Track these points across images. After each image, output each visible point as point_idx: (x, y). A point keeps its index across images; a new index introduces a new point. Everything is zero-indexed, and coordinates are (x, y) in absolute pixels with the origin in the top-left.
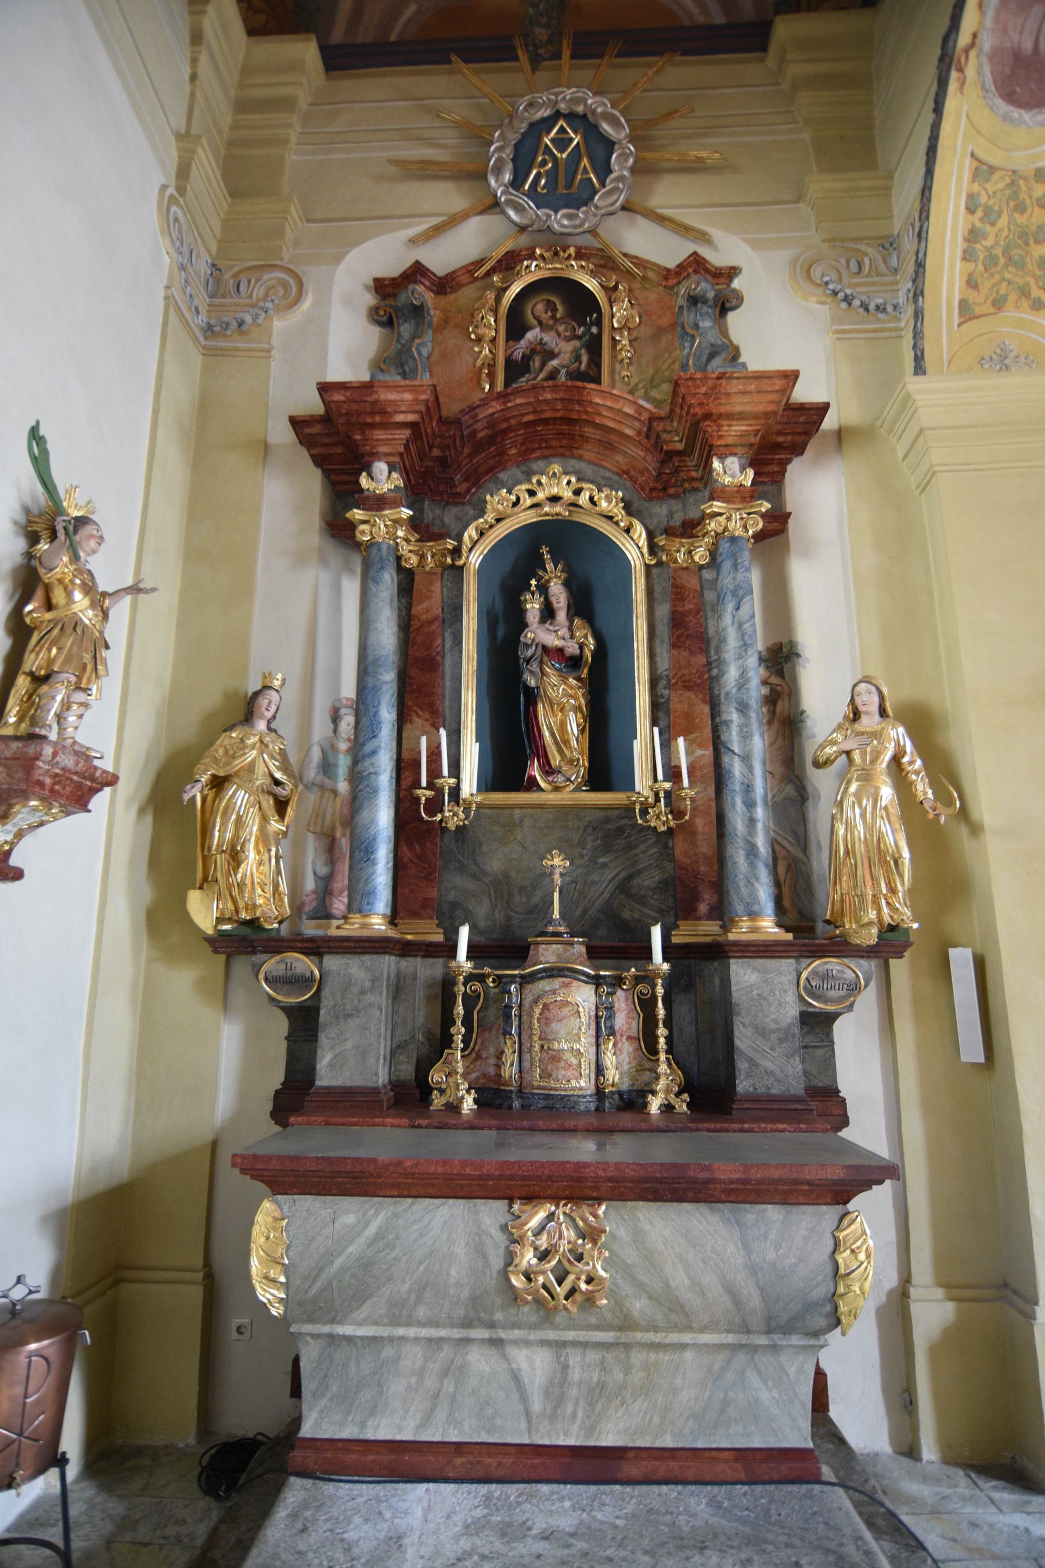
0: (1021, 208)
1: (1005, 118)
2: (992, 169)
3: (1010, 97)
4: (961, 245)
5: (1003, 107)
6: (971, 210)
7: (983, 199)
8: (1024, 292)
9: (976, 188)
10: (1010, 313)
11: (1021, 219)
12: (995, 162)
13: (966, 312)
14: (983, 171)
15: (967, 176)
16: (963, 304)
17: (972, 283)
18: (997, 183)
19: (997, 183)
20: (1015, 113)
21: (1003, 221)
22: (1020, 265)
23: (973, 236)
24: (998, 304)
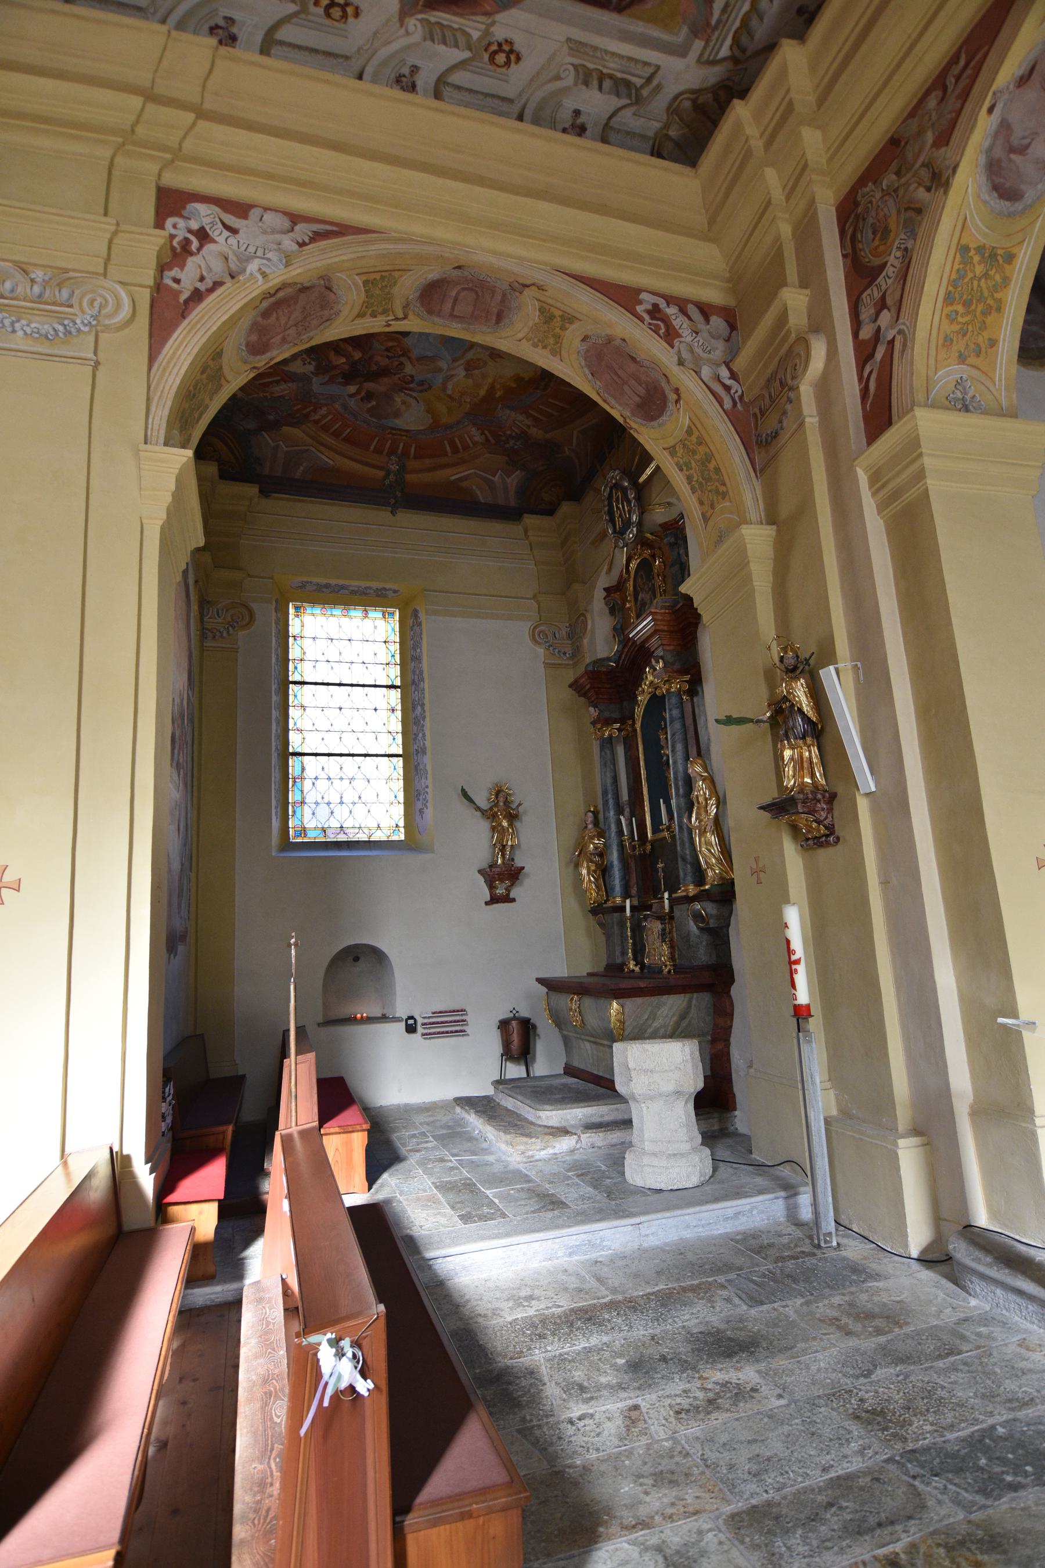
0: (694, 453)
1: (660, 425)
2: (674, 447)
3: (653, 419)
4: (688, 487)
5: (655, 423)
6: (681, 470)
7: (681, 462)
8: (717, 492)
9: (676, 459)
10: (718, 507)
11: (697, 457)
12: (672, 443)
13: (706, 519)
14: (672, 450)
15: (669, 458)
16: (703, 514)
17: (701, 503)
18: (680, 451)
19: (680, 451)
20: (660, 421)
21: (693, 465)
22: (709, 480)
23: (689, 479)
24: (712, 506)
